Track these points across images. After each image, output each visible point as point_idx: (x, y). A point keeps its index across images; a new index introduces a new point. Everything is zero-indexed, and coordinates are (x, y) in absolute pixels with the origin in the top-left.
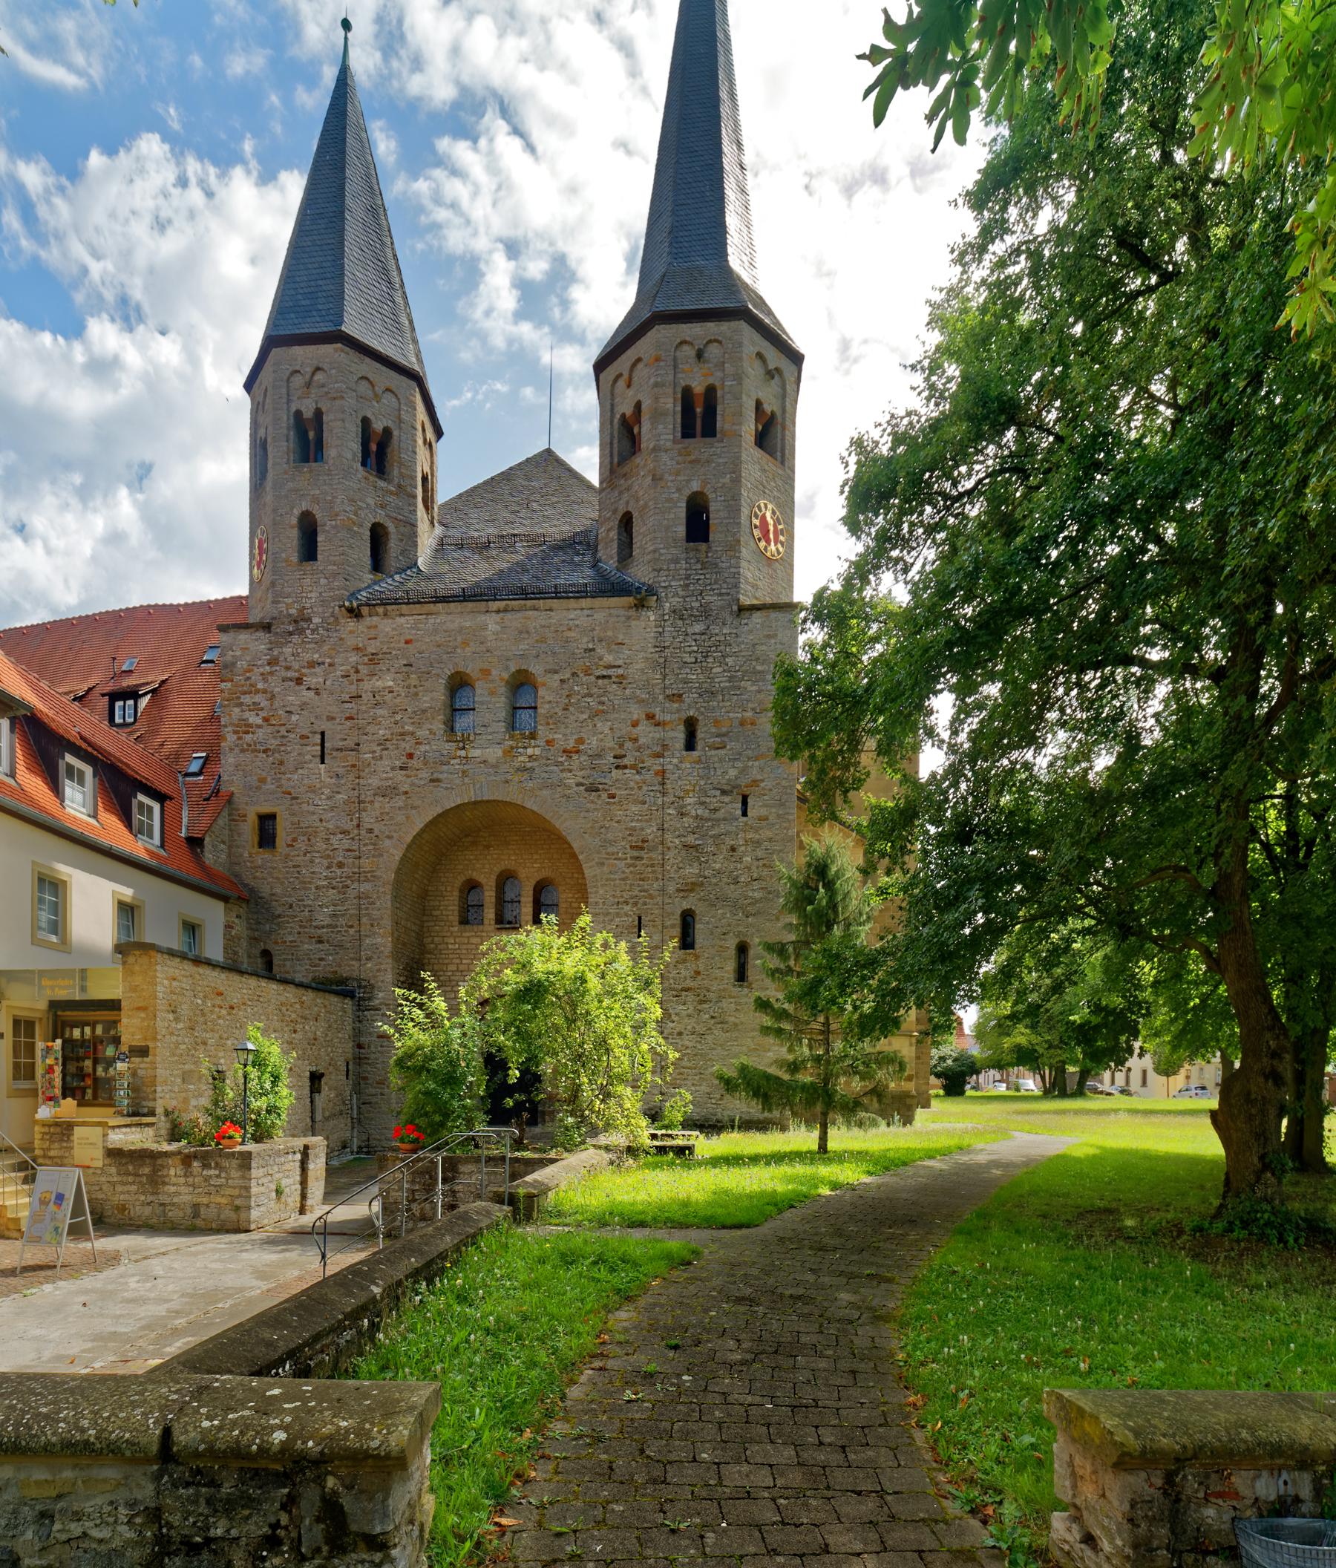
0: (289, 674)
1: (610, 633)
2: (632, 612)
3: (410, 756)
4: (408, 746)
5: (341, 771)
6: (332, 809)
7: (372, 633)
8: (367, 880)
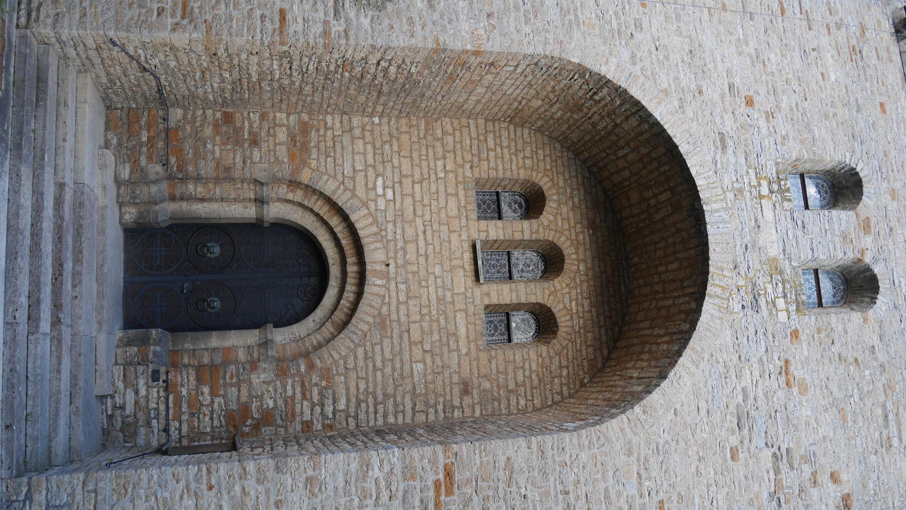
3: (749, 102)
4: (763, 101)
7: (884, 55)
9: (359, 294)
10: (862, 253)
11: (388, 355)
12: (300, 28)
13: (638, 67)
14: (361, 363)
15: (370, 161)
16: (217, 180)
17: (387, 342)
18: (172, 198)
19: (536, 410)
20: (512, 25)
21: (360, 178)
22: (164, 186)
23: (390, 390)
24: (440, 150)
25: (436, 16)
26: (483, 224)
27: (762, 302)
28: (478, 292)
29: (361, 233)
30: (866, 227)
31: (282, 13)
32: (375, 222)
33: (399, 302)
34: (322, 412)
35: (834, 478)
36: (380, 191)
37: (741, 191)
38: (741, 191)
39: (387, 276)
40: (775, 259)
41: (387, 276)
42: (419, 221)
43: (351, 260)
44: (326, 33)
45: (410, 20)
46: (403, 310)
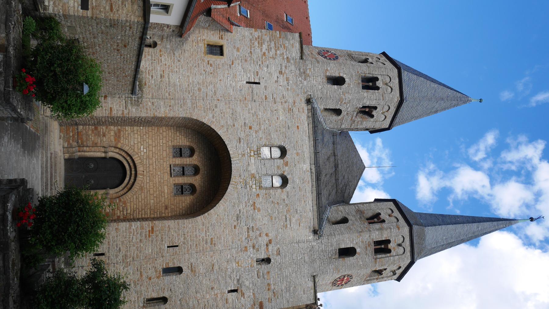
0: (283, 68)
1: (304, 220)
2: (312, 229)
3: (250, 128)
4: (255, 127)
5: (243, 92)
6: (226, 86)
7: (301, 110)
8: (193, 104)
9: (135, 180)
10: (284, 172)
11: (143, 198)
12: (116, 112)
13: (215, 119)
14: (135, 200)
15: (139, 140)
16: (93, 147)
17: (143, 194)
18: (79, 151)
19: (188, 214)
20: (177, 108)
21: (136, 146)
22: (77, 148)
23: (143, 208)
24: (161, 137)
25: (154, 107)
26: (174, 159)
27: (248, 186)
28: (171, 179)
29: (136, 162)
30: (286, 164)
31: (111, 108)
32: (140, 159)
33: (147, 183)
34: (123, 214)
35: (267, 235)
36: (142, 150)
37: (244, 155)
38: (244, 155)
39: (143, 175)
40: (253, 174)
41: (143, 175)
42: (154, 159)
43: (133, 170)
44: (123, 114)
45: (147, 109)
46: (148, 184)
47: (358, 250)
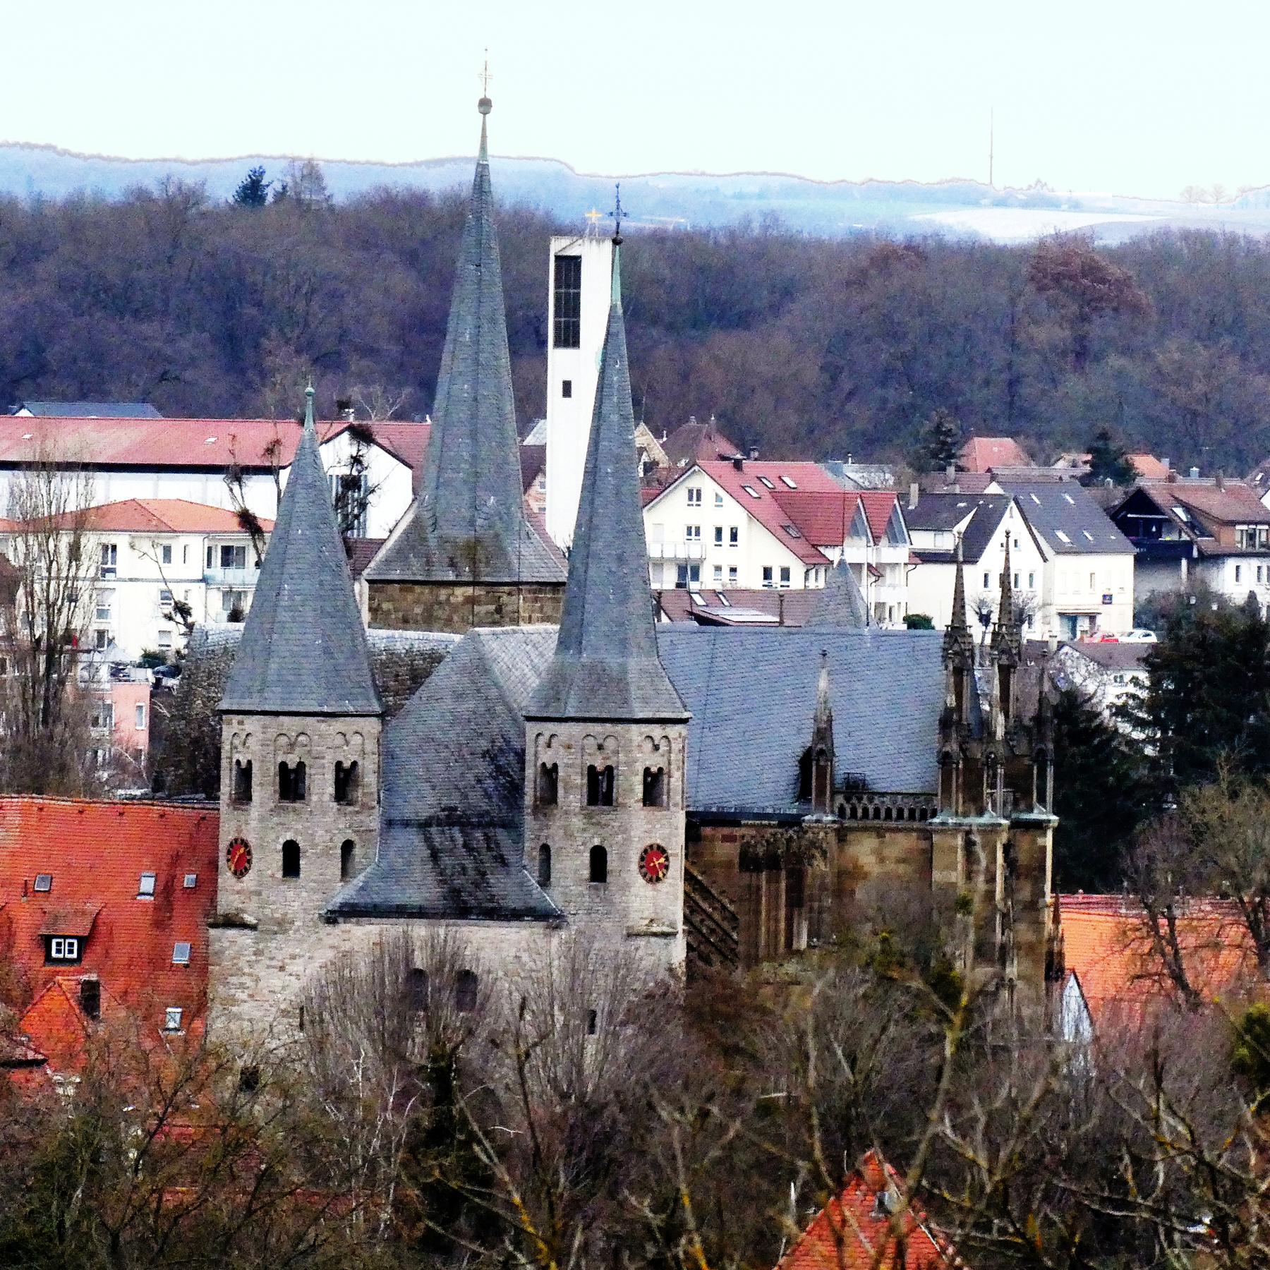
0: (274, 963)
7: (346, 936)
47: (596, 842)
